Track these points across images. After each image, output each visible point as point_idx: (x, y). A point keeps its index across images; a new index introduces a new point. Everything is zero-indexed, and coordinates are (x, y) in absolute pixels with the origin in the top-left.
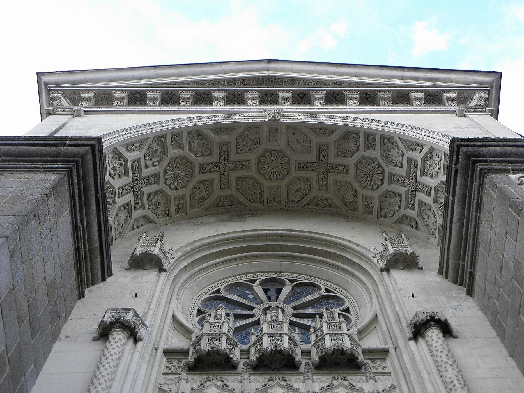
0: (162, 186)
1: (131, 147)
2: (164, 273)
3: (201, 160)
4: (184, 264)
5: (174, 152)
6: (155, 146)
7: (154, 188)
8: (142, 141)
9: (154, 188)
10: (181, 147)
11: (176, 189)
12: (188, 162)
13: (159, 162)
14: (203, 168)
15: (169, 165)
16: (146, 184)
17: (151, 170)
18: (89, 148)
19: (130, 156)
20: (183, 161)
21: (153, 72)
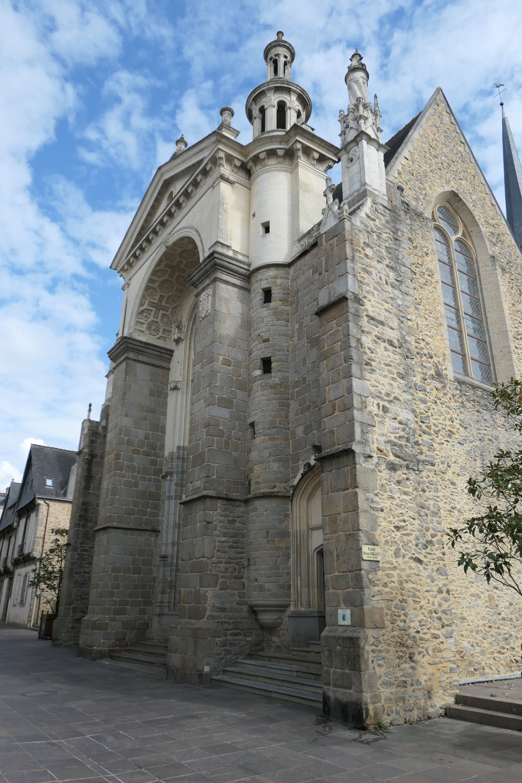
0: (166, 295)
1: (143, 303)
2: (184, 341)
3: (167, 275)
4: (191, 323)
5: (156, 285)
6: (149, 291)
7: (165, 299)
8: (143, 297)
9: (165, 299)
10: (156, 281)
11: (172, 290)
12: (164, 281)
13: (156, 292)
14: (170, 276)
15: (160, 289)
16: (161, 303)
17: (157, 297)
18: (125, 344)
19: (145, 307)
20: (162, 283)
21: (133, 227)
